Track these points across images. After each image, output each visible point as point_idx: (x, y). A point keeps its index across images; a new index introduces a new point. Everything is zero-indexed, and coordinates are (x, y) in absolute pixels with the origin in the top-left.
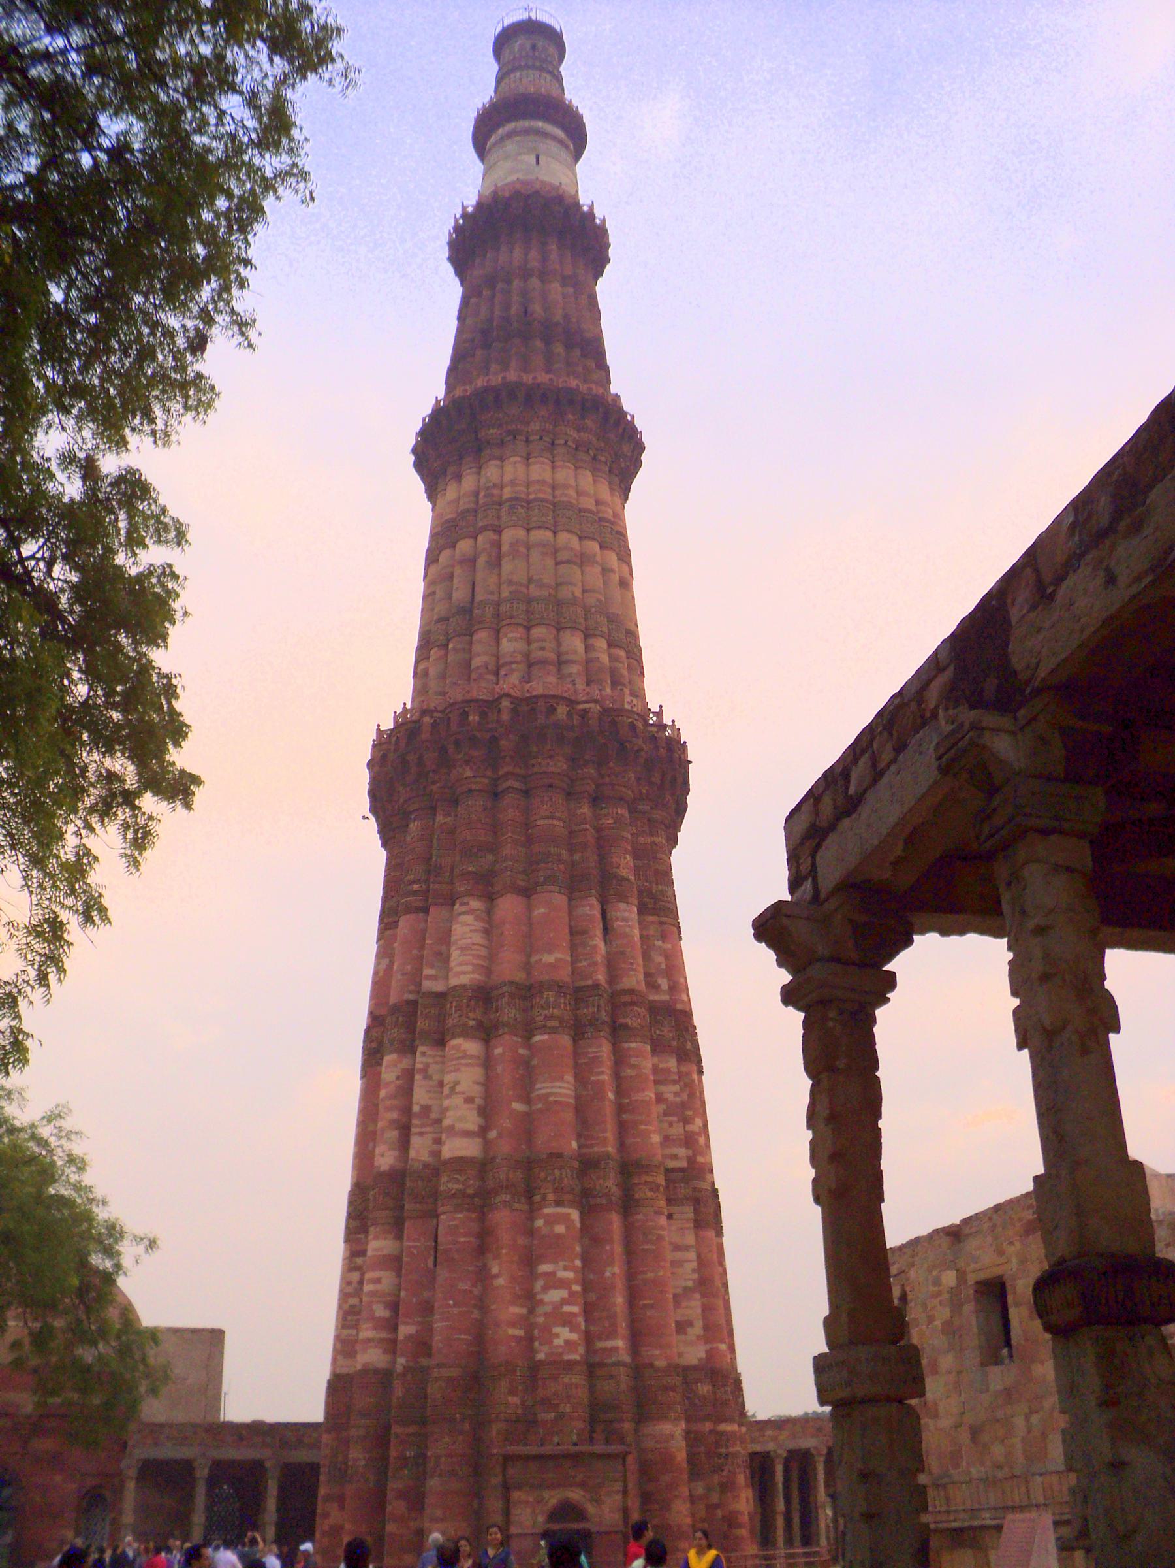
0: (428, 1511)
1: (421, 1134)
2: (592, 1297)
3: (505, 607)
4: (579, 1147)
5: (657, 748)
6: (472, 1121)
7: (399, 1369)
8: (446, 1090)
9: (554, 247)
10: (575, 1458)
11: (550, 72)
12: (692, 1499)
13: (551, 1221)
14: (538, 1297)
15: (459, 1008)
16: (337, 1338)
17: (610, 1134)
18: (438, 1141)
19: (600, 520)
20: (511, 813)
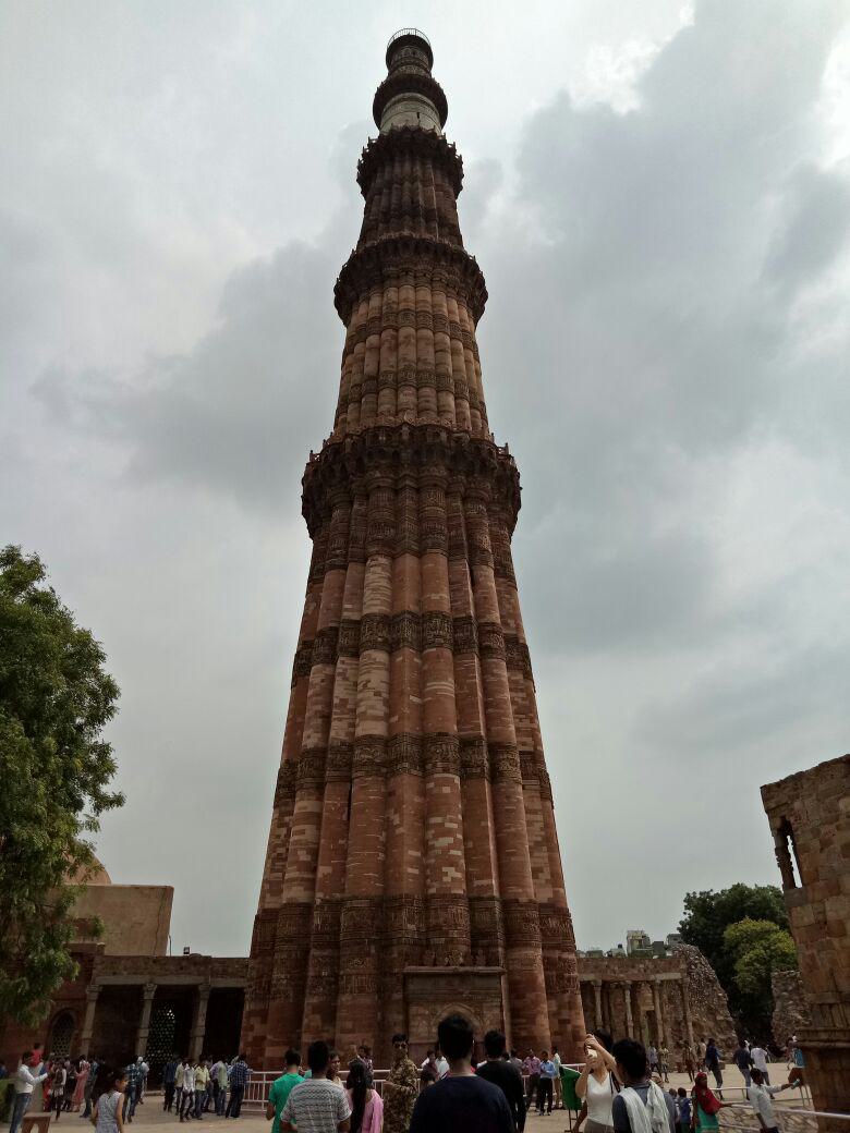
0: (337, 1023)
1: (340, 720)
2: (470, 844)
3: (400, 375)
4: (459, 730)
5: (505, 470)
6: (380, 710)
7: (318, 902)
8: (360, 687)
10: (463, 976)
11: (425, 70)
12: (552, 1015)
13: (440, 783)
14: (430, 843)
15: (370, 629)
16: (264, 881)
18: (353, 725)
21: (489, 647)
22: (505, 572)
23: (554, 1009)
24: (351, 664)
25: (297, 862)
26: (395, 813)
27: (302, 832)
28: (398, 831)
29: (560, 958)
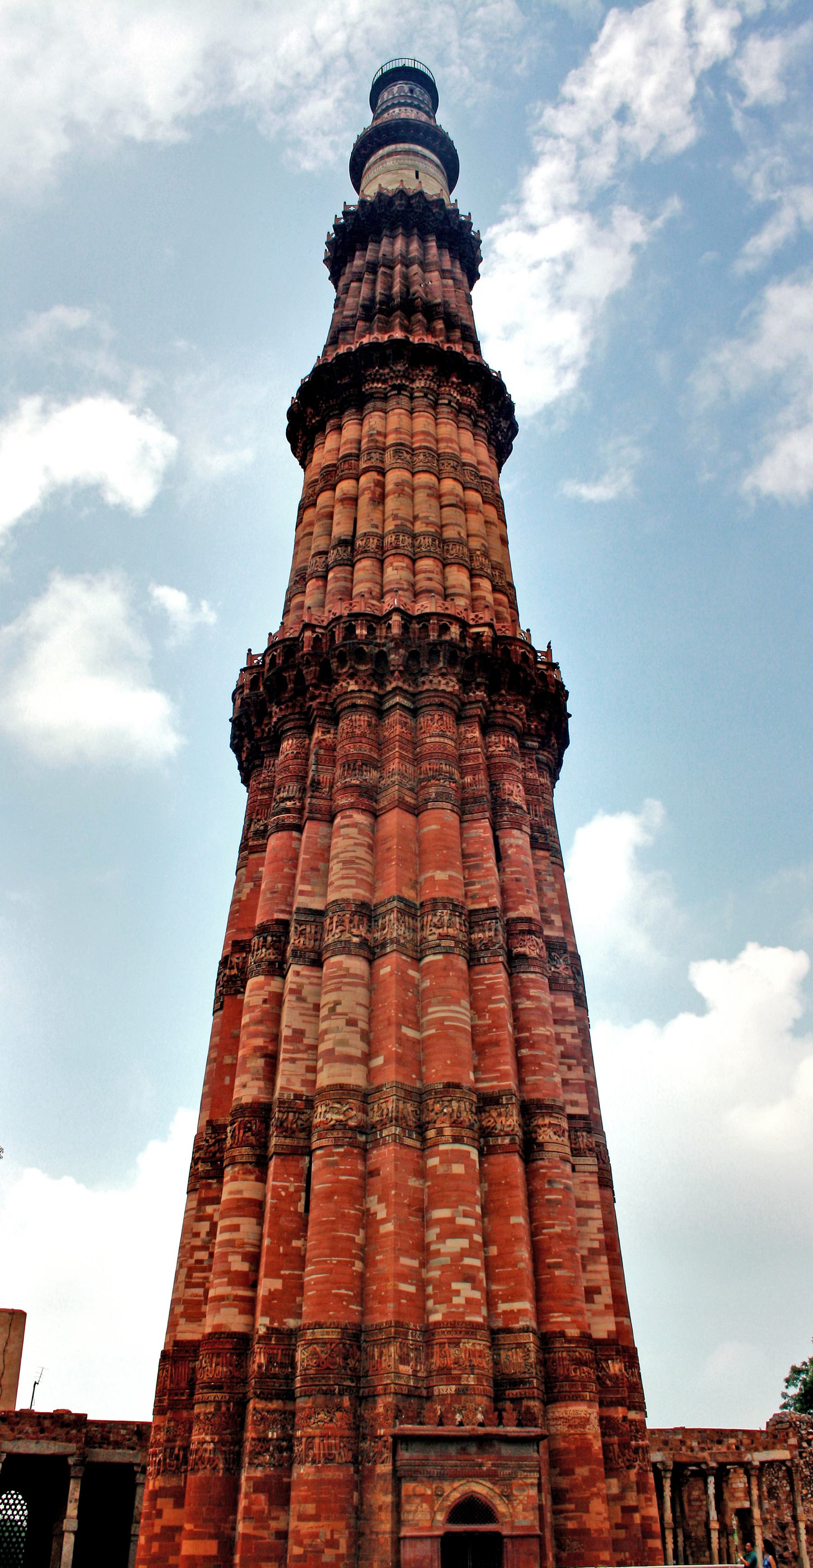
0: (292, 1506)
1: (293, 1061)
3: (389, 539)
4: (477, 1080)
5: (547, 685)
7: (262, 1331)
8: (324, 1012)
9: (434, 244)
10: (484, 1441)
11: (427, 113)
12: (610, 1499)
13: (448, 1159)
14: (433, 1247)
15: (341, 923)
16: (174, 1302)
17: (508, 1066)
18: (313, 1070)
19: (482, 478)
20: (398, 729)
21: (523, 956)
22: (546, 841)
23: (615, 1490)
25: (227, 1272)
26: (380, 1201)
27: (236, 1228)
29: (625, 1418)
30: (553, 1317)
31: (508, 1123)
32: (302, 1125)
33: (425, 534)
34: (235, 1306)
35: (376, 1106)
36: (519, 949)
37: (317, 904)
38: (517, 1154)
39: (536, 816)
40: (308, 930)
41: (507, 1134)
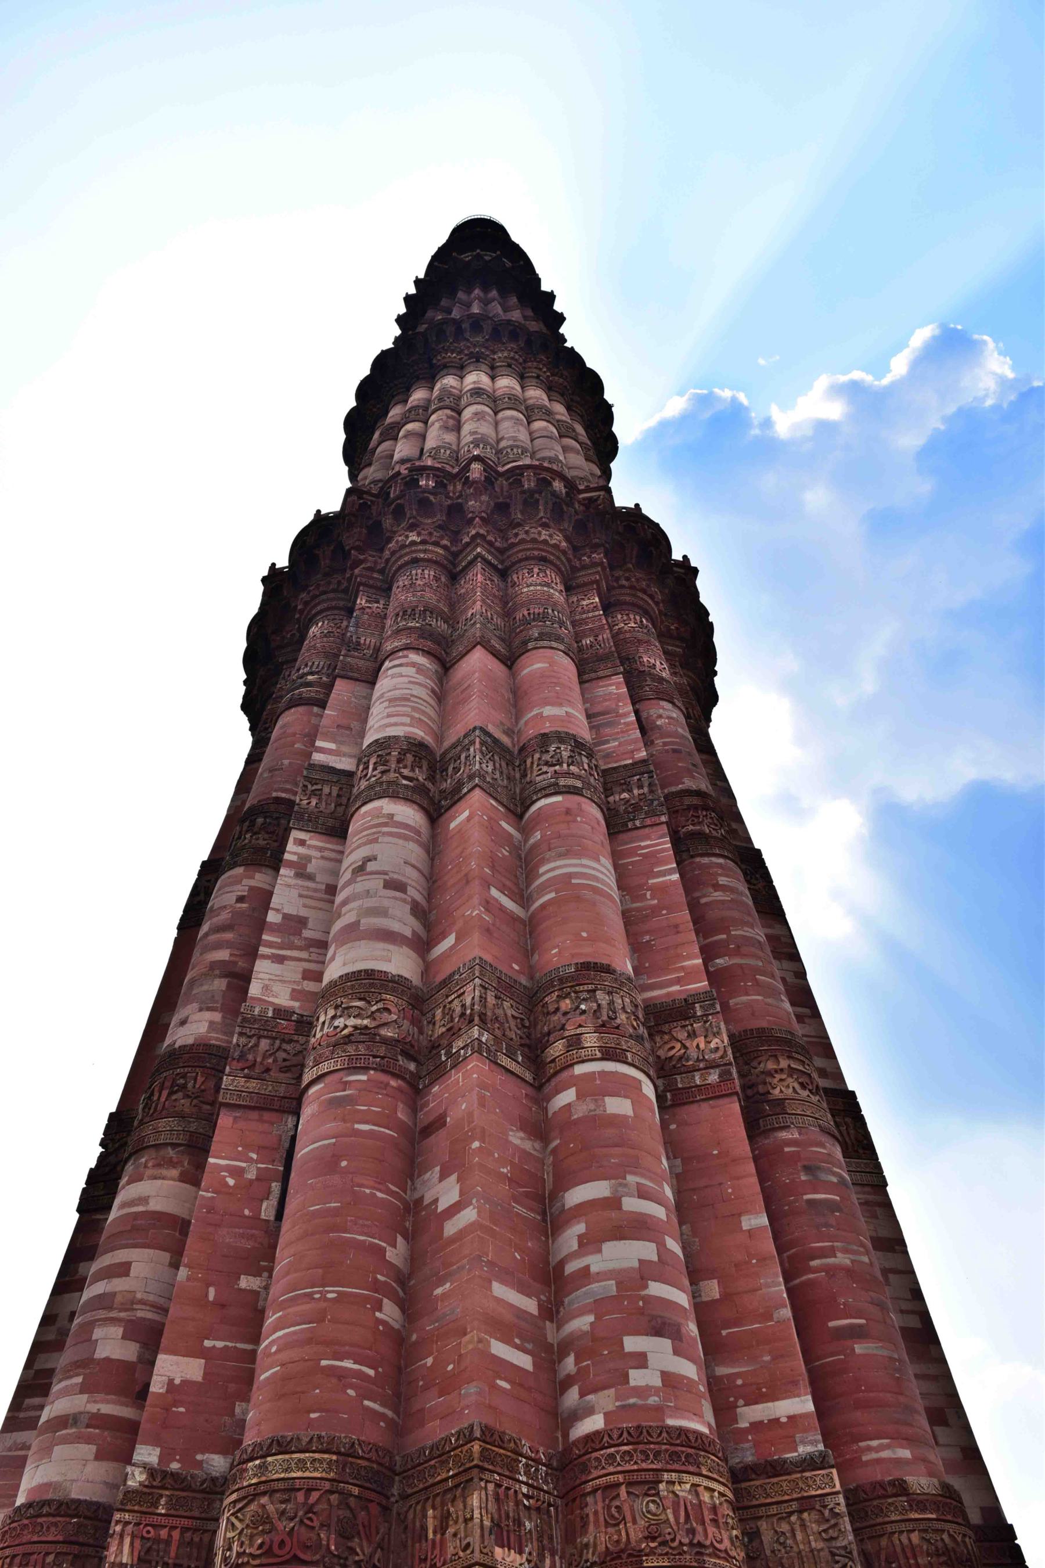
1: (280, 960)
2: (712, 1289)
7: (137, 1478)
15: (383, 761)
24: (321, 849)
26: (443, 1176)
27: (123, 1270)
28: (451, 1228)
30: (870, 1449)
31: (712, 1045)
32: (285, 1060)
33: (512, 448)
34: (89, 1440)
35: (439, 1012)
36: (691, 827)
37: (345, 764)
38: (736, 1098)
39: (690, 718)
40: (326, 790)
41: (711, 1066)
